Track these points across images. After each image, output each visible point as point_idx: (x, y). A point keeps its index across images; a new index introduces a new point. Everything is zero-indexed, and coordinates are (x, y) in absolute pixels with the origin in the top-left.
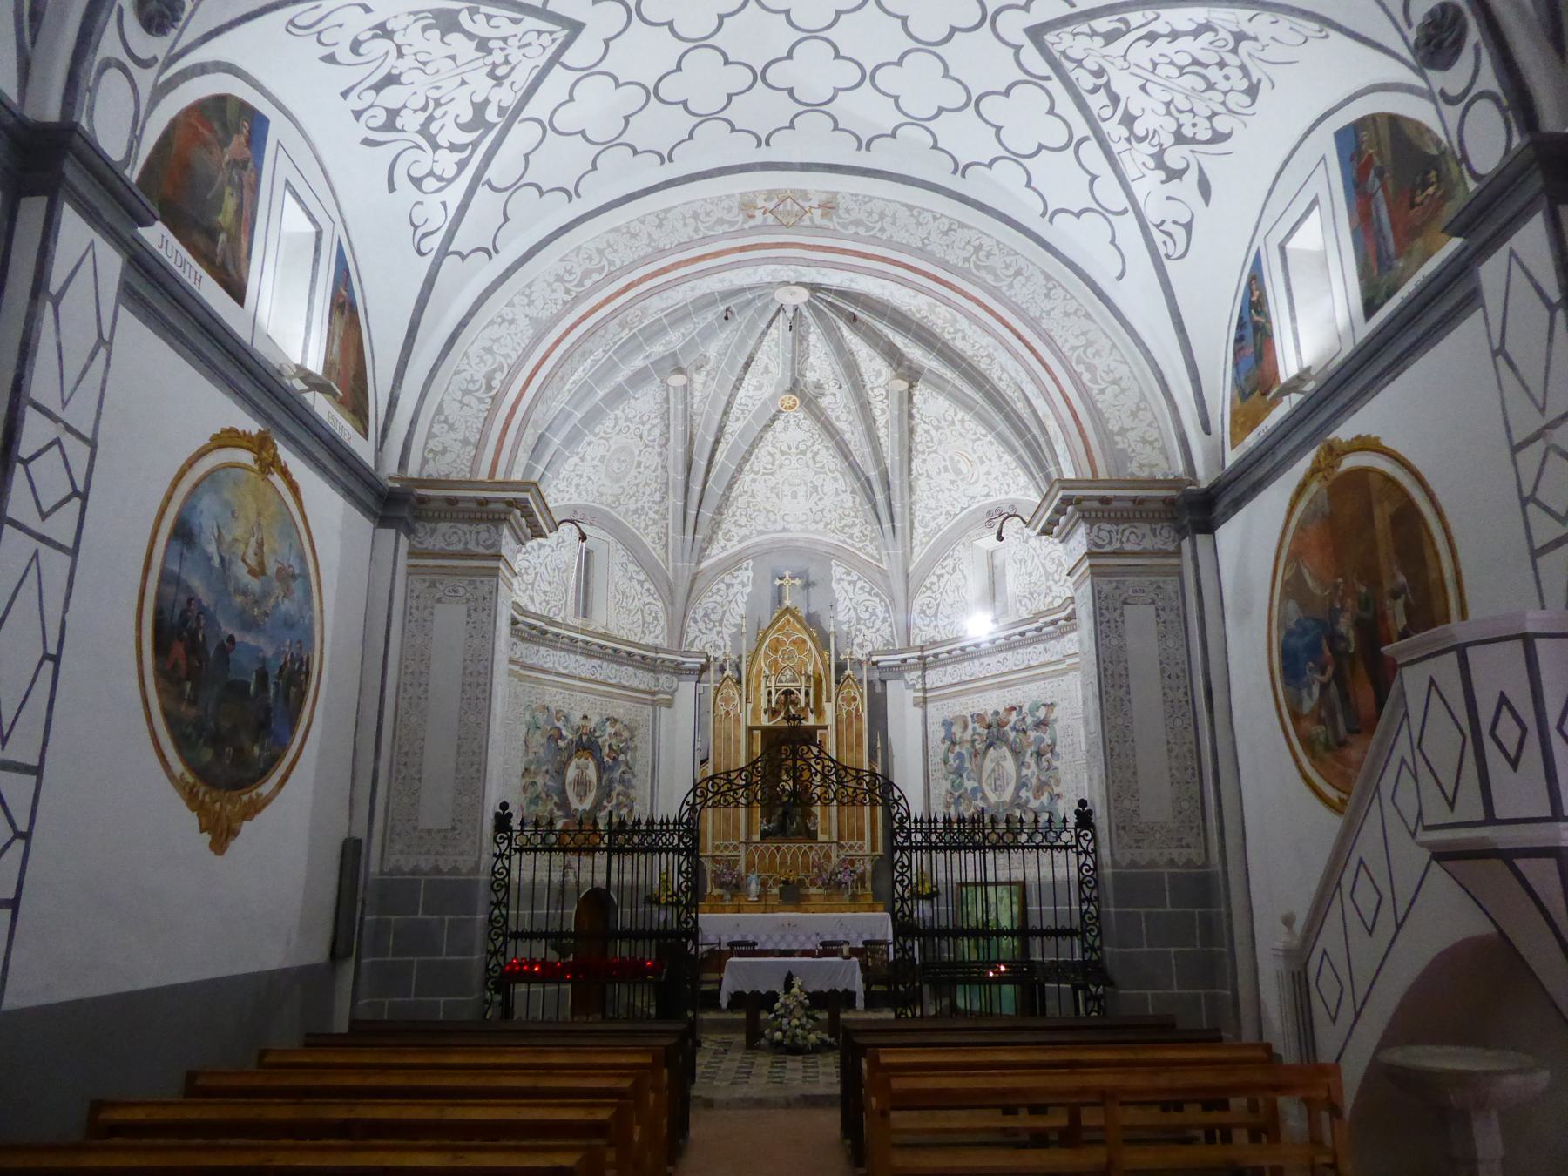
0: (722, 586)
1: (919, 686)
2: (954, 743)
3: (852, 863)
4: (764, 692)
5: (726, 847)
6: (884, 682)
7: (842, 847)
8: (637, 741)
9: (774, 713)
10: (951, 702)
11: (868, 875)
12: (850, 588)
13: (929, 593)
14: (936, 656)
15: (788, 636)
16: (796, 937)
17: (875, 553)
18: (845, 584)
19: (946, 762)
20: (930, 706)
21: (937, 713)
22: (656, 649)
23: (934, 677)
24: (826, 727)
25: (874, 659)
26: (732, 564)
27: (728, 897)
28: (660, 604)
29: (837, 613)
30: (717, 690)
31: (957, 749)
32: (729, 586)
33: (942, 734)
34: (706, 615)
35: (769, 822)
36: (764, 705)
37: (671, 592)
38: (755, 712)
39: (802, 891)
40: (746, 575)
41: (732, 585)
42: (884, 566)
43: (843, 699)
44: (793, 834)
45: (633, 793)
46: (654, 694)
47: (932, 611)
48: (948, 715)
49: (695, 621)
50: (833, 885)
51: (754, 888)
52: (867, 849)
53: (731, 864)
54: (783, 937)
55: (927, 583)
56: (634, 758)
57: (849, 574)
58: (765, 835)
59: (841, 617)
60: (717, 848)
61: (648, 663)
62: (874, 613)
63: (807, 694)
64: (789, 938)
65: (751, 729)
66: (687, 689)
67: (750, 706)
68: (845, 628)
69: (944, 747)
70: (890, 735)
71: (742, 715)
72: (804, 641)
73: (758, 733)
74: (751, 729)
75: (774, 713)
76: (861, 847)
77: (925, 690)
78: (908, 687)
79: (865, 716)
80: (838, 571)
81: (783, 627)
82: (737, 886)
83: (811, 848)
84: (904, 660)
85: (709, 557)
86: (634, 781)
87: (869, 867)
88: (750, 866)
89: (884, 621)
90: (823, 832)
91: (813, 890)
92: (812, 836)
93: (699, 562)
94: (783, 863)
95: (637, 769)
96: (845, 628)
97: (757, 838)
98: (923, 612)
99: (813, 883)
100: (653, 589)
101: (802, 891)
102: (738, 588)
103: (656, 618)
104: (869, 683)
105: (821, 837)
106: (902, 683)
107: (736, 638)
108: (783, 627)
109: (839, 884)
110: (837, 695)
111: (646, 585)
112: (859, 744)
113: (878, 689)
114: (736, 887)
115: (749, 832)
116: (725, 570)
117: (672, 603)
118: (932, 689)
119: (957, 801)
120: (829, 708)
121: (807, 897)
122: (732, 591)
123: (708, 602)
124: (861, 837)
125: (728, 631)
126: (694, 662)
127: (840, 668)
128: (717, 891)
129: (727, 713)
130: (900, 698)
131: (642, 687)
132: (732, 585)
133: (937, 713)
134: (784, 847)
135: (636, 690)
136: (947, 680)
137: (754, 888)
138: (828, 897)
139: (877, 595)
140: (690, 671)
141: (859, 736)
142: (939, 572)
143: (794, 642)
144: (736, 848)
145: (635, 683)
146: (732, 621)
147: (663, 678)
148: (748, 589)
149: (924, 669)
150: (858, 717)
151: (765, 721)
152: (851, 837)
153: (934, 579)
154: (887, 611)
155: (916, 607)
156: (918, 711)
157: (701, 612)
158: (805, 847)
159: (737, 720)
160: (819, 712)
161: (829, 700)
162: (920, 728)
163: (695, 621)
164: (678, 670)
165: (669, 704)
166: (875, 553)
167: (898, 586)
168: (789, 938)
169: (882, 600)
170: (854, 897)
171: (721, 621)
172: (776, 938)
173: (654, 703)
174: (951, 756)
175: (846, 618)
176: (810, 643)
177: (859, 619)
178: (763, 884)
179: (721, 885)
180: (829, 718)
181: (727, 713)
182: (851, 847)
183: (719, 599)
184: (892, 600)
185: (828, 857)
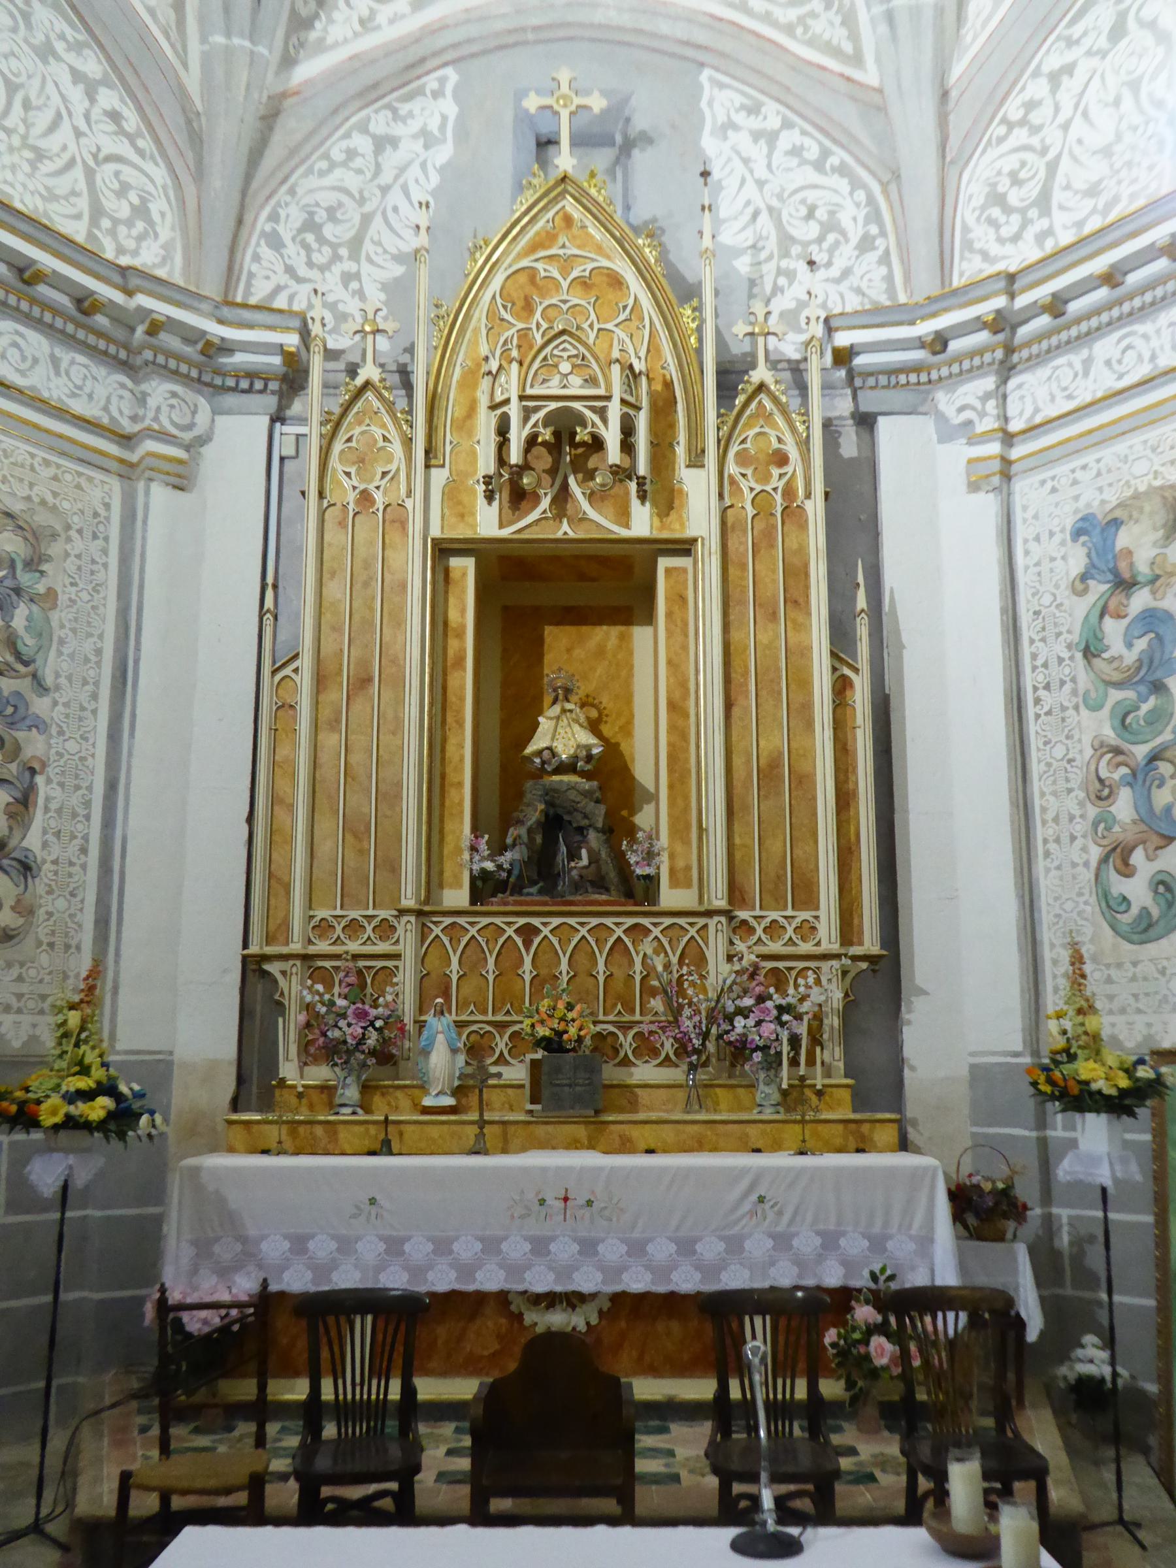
0: (362, 143)
1: (988, 424)
2: (1125, 584)
3: (779, 979)
4: (486, 423)
5: (354, 927)
6: (866, 422)
7: (744, 928)
8: (55, 576)
9: (519, 498)
10: (1109, 454)
11: (833, 1022)
12: (757, 152)
13: (1020, 136)
14: (1056, 306)
15: (565, 264)
16: (589, 1247)
17: (839, 36)
18: (742, 140)
19: (1090, 651)
20: (1026, 490)
21: (1049, 504)
22: (127, 277)
23: (1036, 392)
24: (684, 548)
25: (843, 339)
26: (395, 77)
27: (352, 1093)
28: (159, 173)
29: (717, 223)
30: (334, 425)
31: (1140, 600)
32: (383, 143)
33: (1077, 560)
34: (310, 225)
35: (499, 848)
36: (486, 463)
37: (196, 139)
38: (453, 493)
39: (610, 1073)
40: (436, 108)
41: (394, 142)
42: (870, 76)
43: (743, 458)
44: (578, 886)
45: (34, 745)
46: (126, 440)
47: (1032, 190)
48: (1098, 497)
49: (276, 243)
50: (723, 1055)
51: (441, 1061)
52: (827, 936)
53: (366, 979)
54: (540, 1246)
55: (1013, 110)
56: (43, 634)
57: (753, 110)
58: (484, 888)
59: (727, 237)
60: (323, 928)
61: (100, 323)
62: (831, 226)
63: (628, 430)
64: (564, 1249)
65: (443, 550)
66: (239, 438)
67: (439, 477)
68: (743, 265)
69: (1082, 607)
70: (891, 577)
71: (414, 505)
72: (616, 282)
73: (465, 567)
74: (443, 550)
75: (519, 498)
76: (807, 930)
77: (1009, 439)
78: (947, 432)
79: (815, 509)
80: (720, 99)
81: (548, 239)
82: (385, 1057)
83: (637, 931)
84: (940, 342)
85: (321, 47)
86: (40, 706)
87: (837, 996)
88: (434, 990)
89: (866, 245)
90: (675, 883)
91: (644, 1072)
92: (638, 891)
93: (288, 61)
94: (543, 981)
95: (51, 666)
96: (743, 265)
97: (457, 896)
98: (999, 199)
99: (647, 1048)
100: (132, 120)
101: (610, 1073)
102: (410, 147)
103: (141, 211)
104: (827, 424)
105: (670, 897)
106: (924, 425)
107: (398, 291)
108: (548, 239)
109: (740, 1051)
110: (724, 445)
111: (108, 98)
112: (797, 601)
113: (849, 446)
114: (383, 1058)
115: (433, 881)
116: (371, 94)
117: (200, 174)
118: (1032, 430)
119: (1143, 776)
120: (697, 487)
121: (627, 1096)
122: (391, 159)
123: (315, 187)
124: (806, 895)
125: (377, 273)
126: (257, 345)
127: (730, 378)
128: (320, 1073)
129: (365, 498)
130: (923, 473)
131: (78, 407)
132: (394, 142)
133: (1049, 504)
134: (546, 926)
135: (61, 413)
136: (1104, 381)
137: (441, 1061)
138: (699, 1096)
139: (842, 170)
140: (250, 381)
141: (797, 573)
142: (1053, 61)
143: (584, 283)
144: (385, 929)
145: (56, 390)
146: (392, 244)
147: (159, 390)
148: (443, 154)
149: (1006, 370)
150: (793, 513)
151: (487, 521)
152: (773, 896)
153: (1038, 89)
154: (875, 216)
155: (973, 187)
156: (987, 504)
157: (293, 217)
158: (618, 926)
159: (396, 518)
160: (664, 495)
161: (696, 460)
162: (992, 554)
163: (276, 243)
164: (208, 370)
165: (181, 480)
166: (839, 36)
167: (914, 121)
168: (564, 1249)
169: (856, 184)
170: (792, 1098)
171: (356, 244)
172: (516, 1248)
173: (128, 471)
174: (1113, 629)
175: (748, 238)
176: (635, 285)
177: (786, 240)
178: (476, 1050)
179: (333, 1052)
180: (699, 516)
181: (365, 498)
182: (773, 929)
183: (352, 181)
184: (893, 178)
185: (695, 957)
